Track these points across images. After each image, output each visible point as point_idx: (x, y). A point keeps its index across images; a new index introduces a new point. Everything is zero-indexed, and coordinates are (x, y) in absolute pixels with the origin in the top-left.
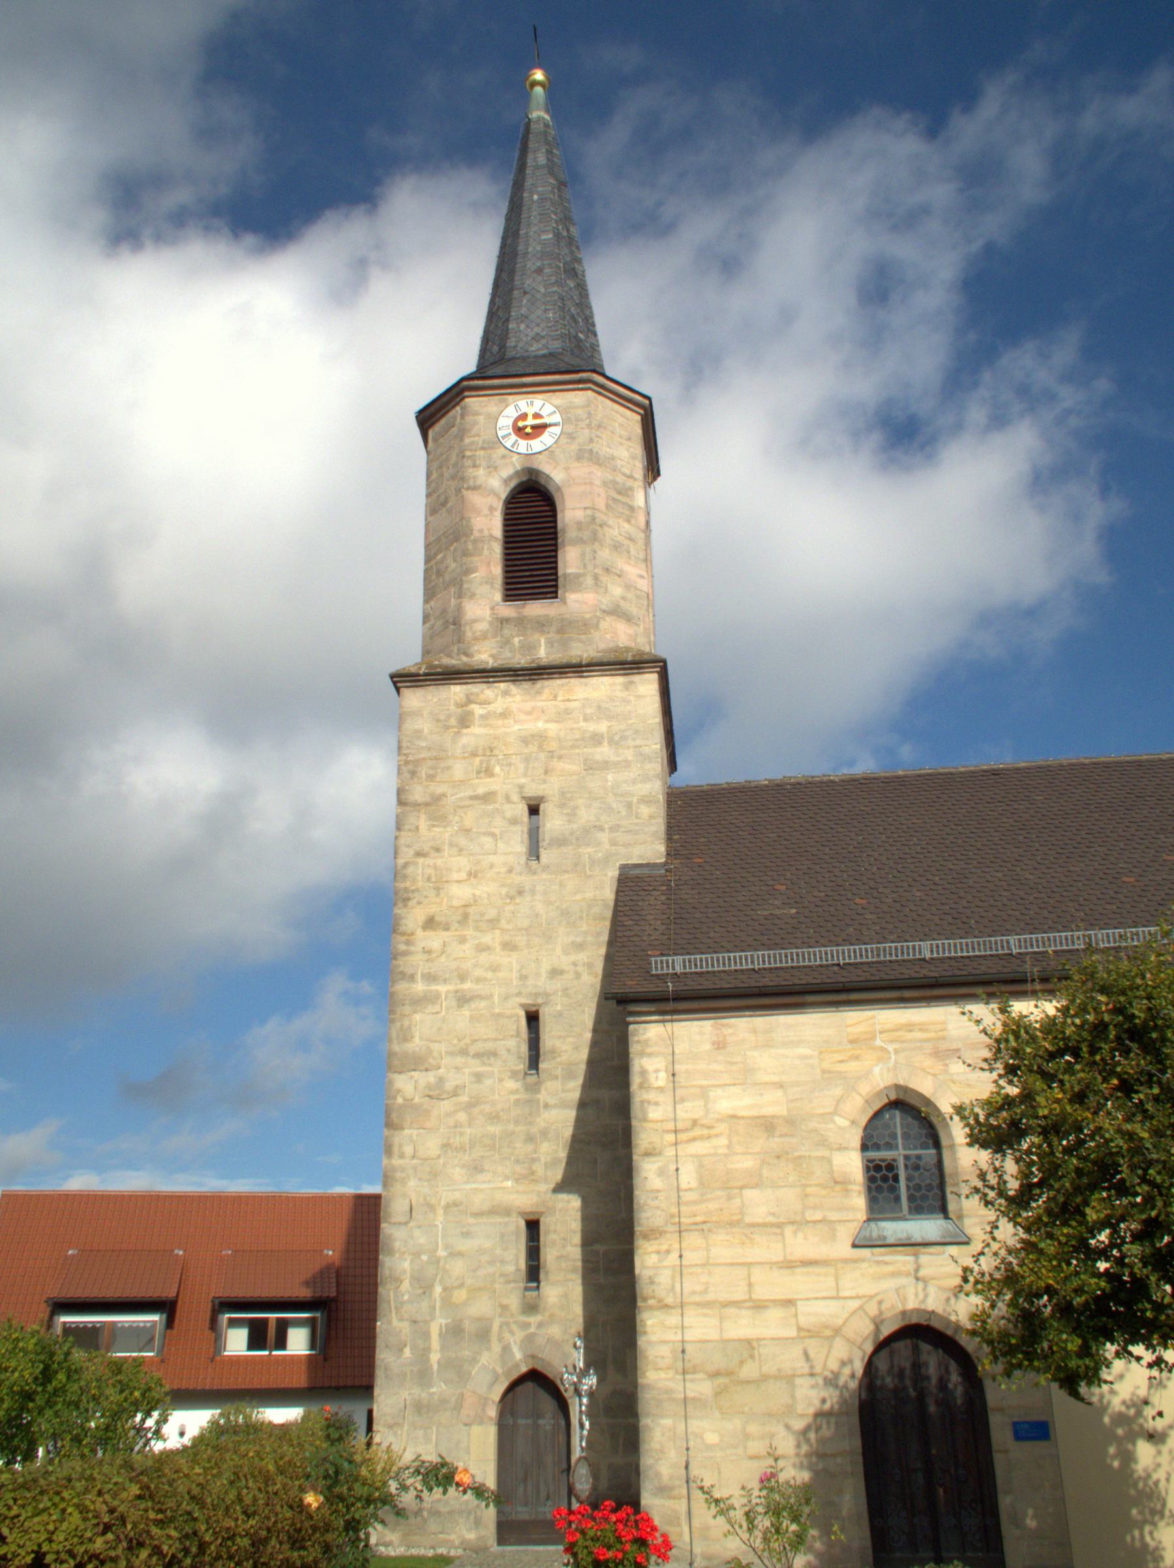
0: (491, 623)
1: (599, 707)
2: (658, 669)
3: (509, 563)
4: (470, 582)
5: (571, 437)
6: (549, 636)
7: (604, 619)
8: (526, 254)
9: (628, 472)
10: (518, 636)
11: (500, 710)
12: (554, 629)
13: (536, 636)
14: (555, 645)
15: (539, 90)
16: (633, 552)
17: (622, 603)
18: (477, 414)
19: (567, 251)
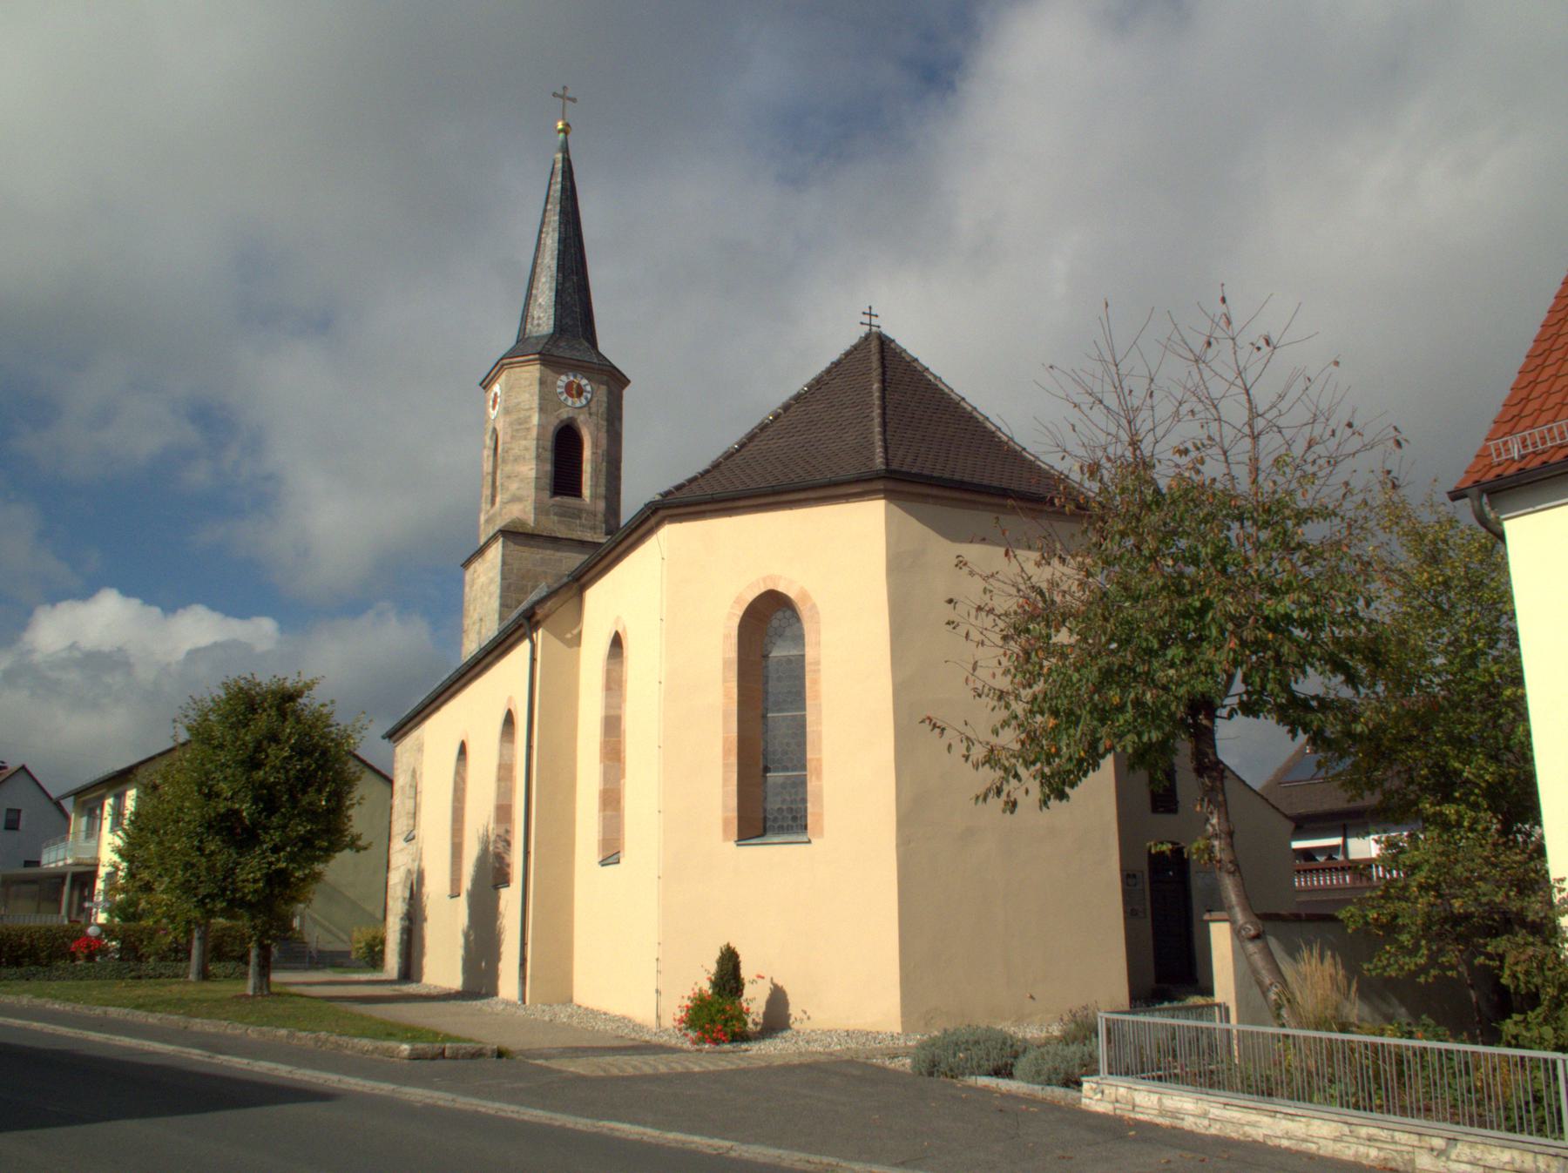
9: (527, 407)
16: (527, 457)
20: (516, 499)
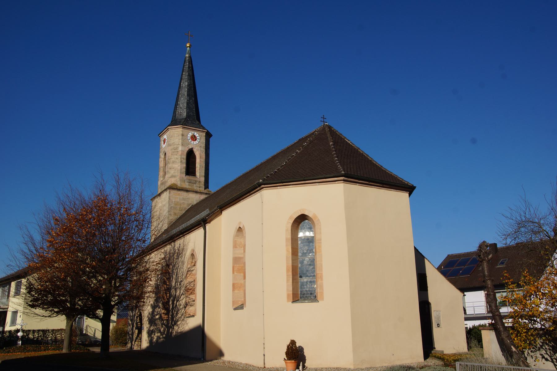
9: (177, 144)
16: (177, 161)
17: (174, 174)
20: (173, 176)
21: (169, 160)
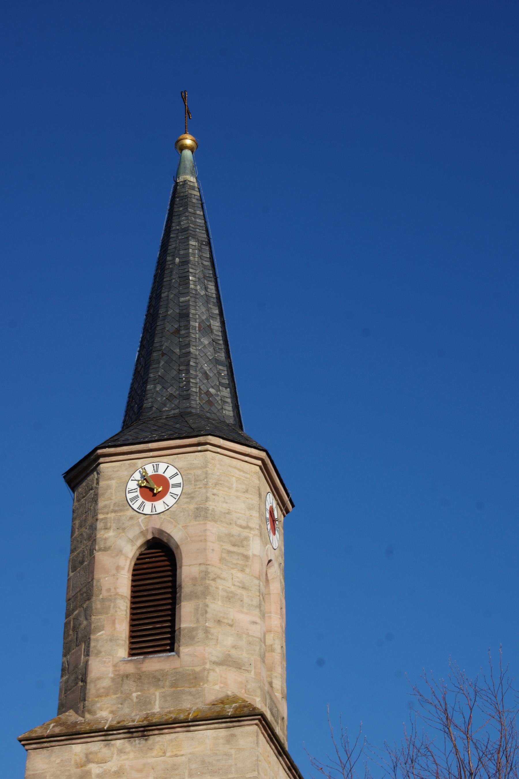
0: (113, 680)
1: (203, 762)
2: (257, 722)
3: (135, 617)
4: (97, 640)
5: (190, 497)
6: (163, 690)
7: (213, 670)
8: (165, 317)
9: (244, 523)
10: (136, 691)
11: (114, 769)
12: (168, 683)
13: (152, 690)
14: (169, 698)
15: (187, 153)
16: (246, 600)
17: (233, 652)
18: (110, 478)
19: (203, 309)
21: (212, 583)
